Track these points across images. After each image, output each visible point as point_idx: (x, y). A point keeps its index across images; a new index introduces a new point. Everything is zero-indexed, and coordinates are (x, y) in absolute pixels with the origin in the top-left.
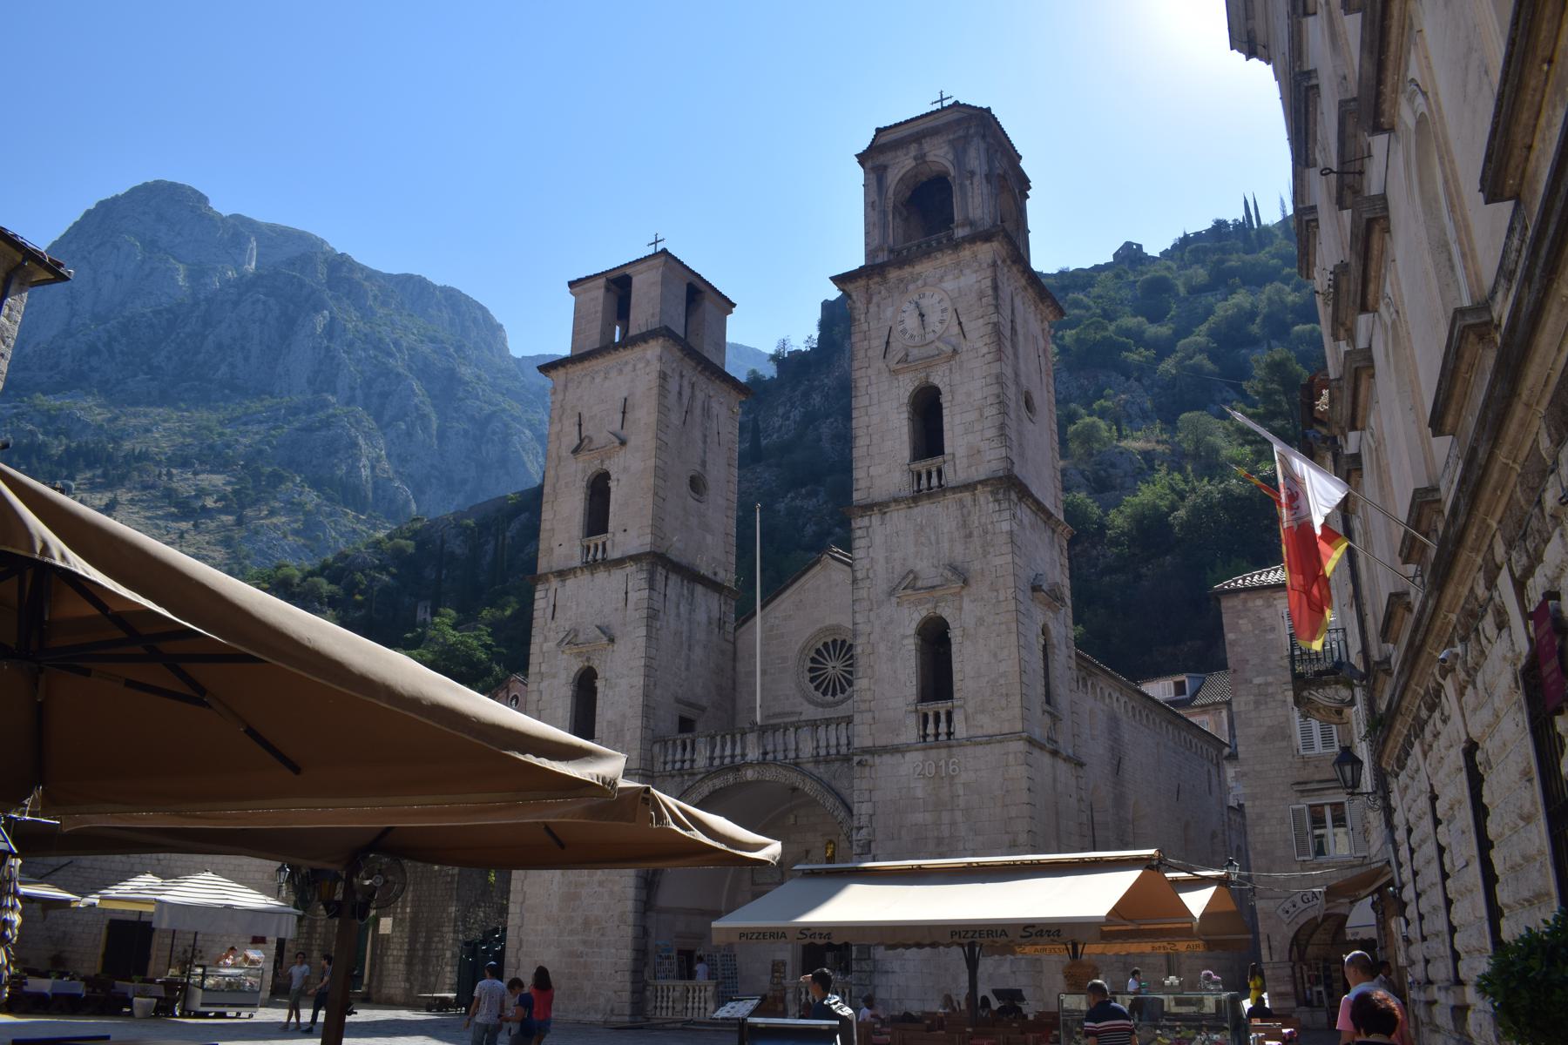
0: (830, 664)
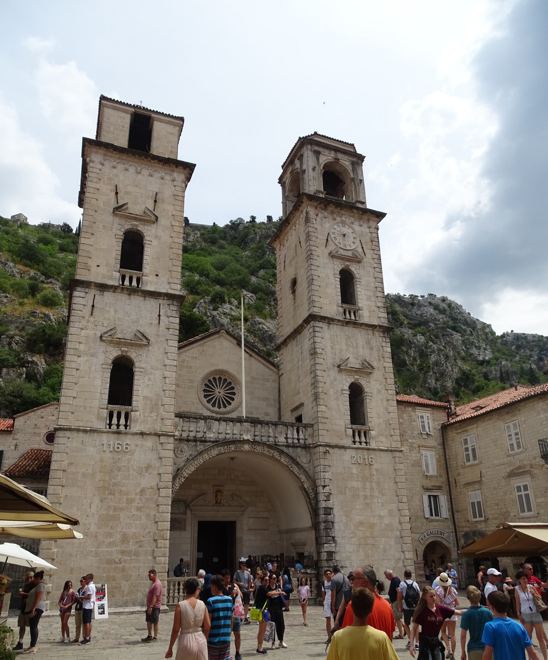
0: (217, 390)
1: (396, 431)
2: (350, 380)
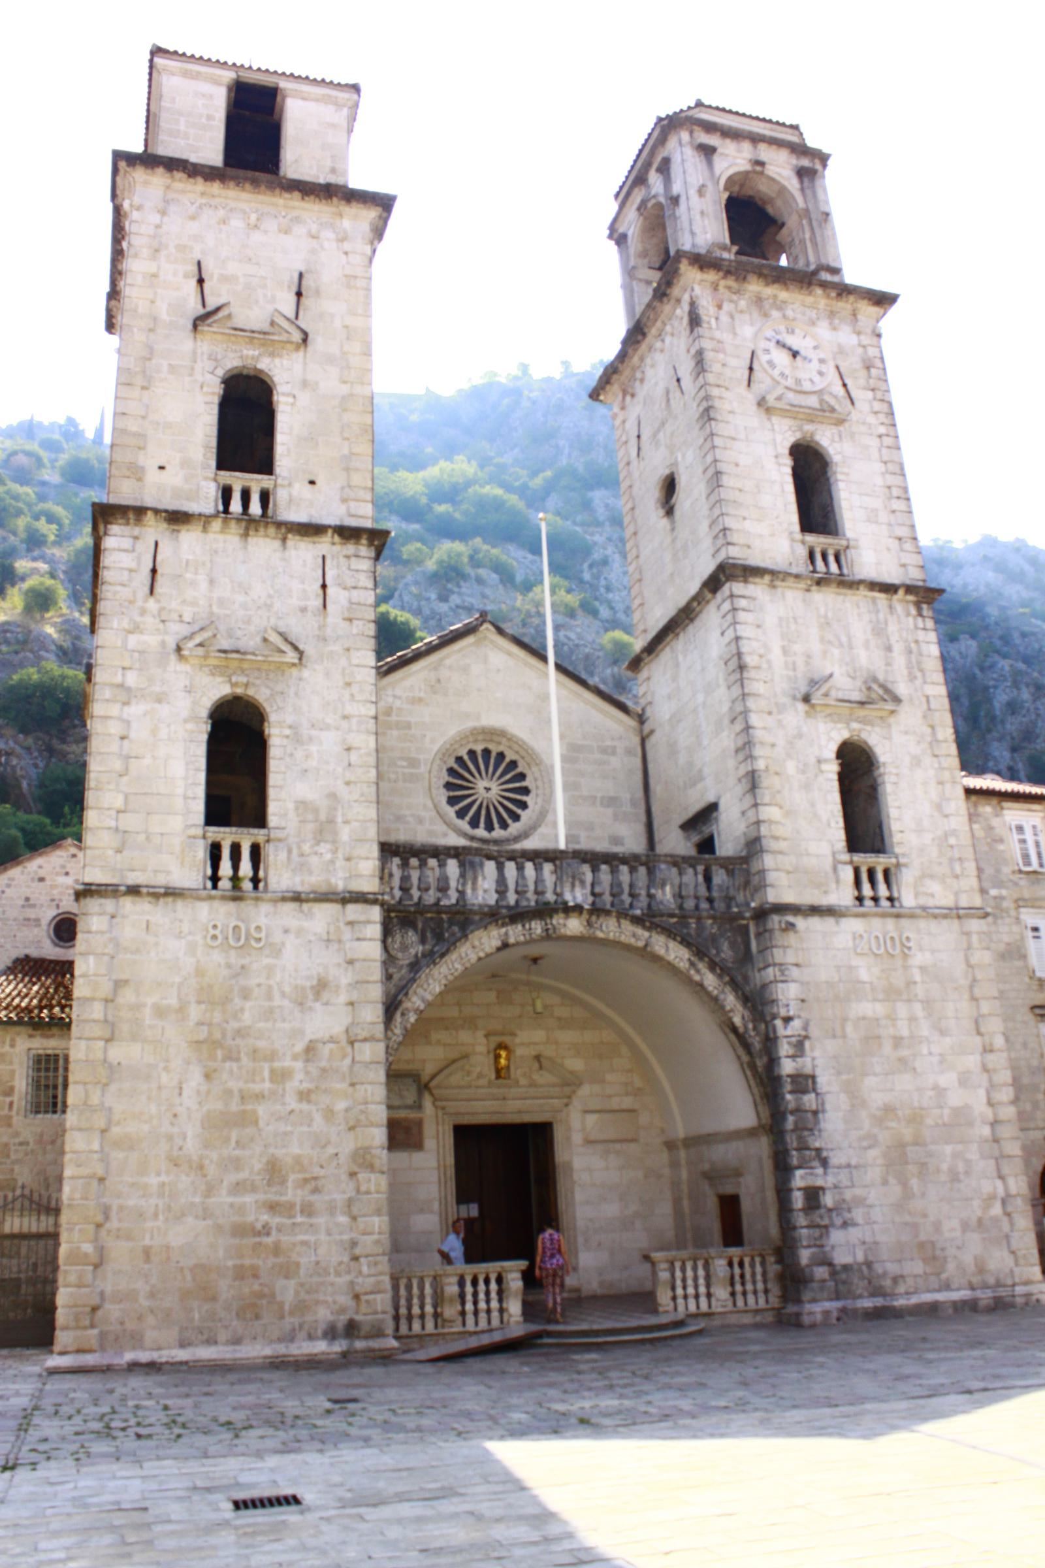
0: (481, 784)
2: (840, 734)
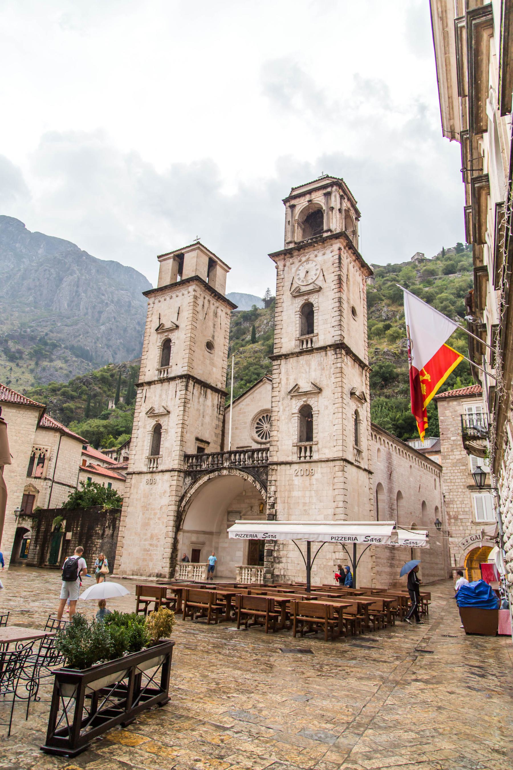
0: (265, 425)
1: (338, 441)
2: (301, 403)
